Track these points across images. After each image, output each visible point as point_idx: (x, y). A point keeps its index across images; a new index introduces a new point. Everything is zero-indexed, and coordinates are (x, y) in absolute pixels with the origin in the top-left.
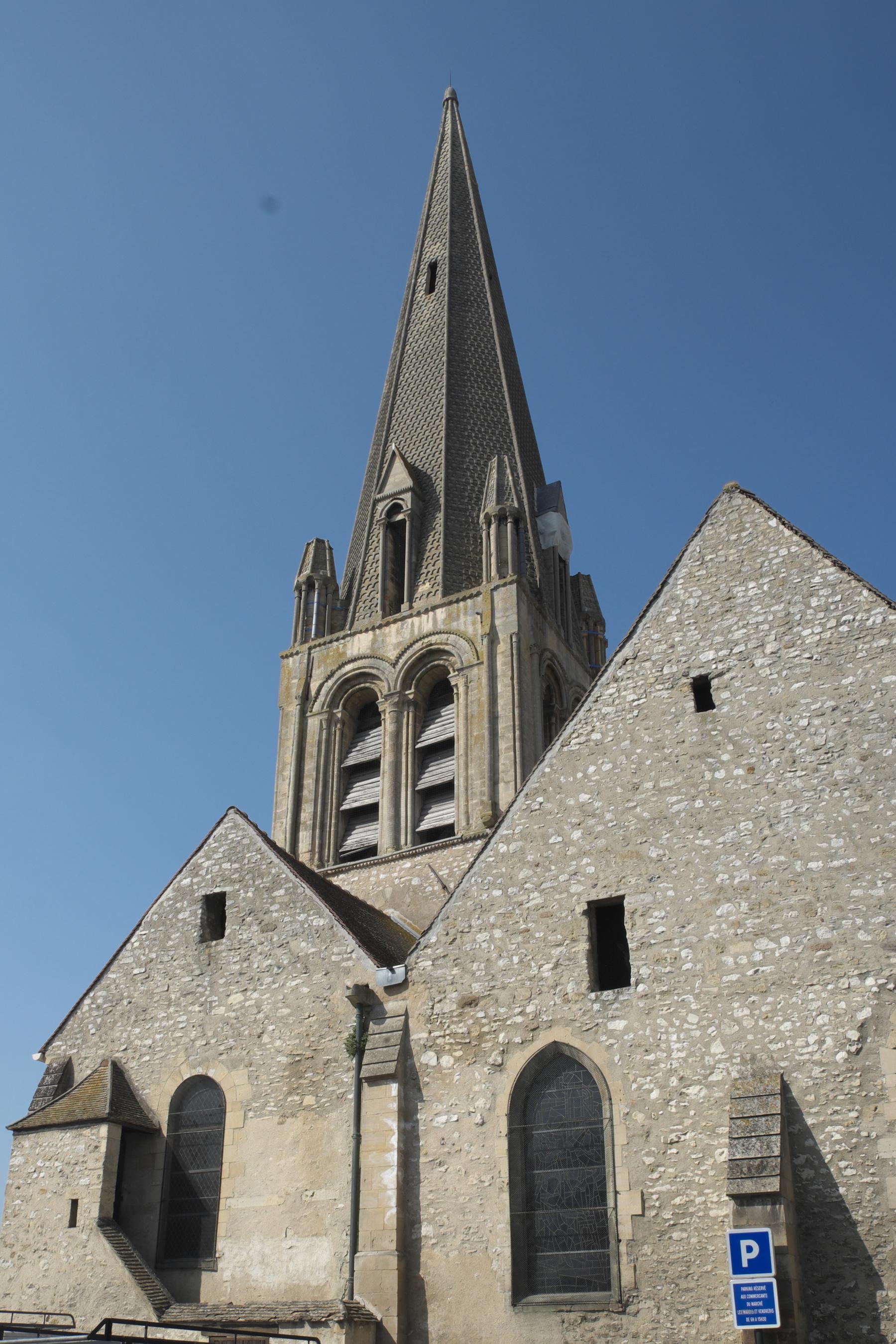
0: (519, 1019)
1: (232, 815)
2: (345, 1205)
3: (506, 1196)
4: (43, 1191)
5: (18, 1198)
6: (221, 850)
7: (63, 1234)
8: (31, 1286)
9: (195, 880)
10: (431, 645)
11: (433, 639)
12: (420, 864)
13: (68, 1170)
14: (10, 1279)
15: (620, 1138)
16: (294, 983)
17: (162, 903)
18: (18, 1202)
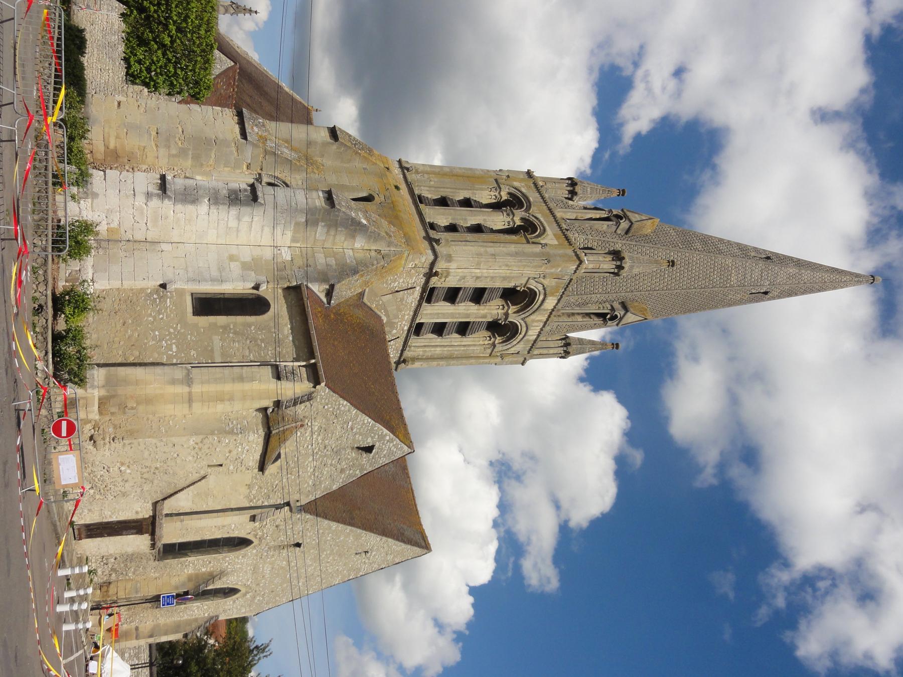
0: (265, 535)
1: (410, 451)
2: (204, 508)
3: (200, 539)
4: (230, 452)
5: (229, 441)
6: (395, 450)
7: (205, 463)
8: (178, 455)
9: (386, 442)
10: (520, 334)
11: (521, 336)
12: (403, 333)
13: (239, 461)
14: (183, 446)
15: (214, 555)
16: (310, 483)
17: (382, 429)
18: (227, 441)
